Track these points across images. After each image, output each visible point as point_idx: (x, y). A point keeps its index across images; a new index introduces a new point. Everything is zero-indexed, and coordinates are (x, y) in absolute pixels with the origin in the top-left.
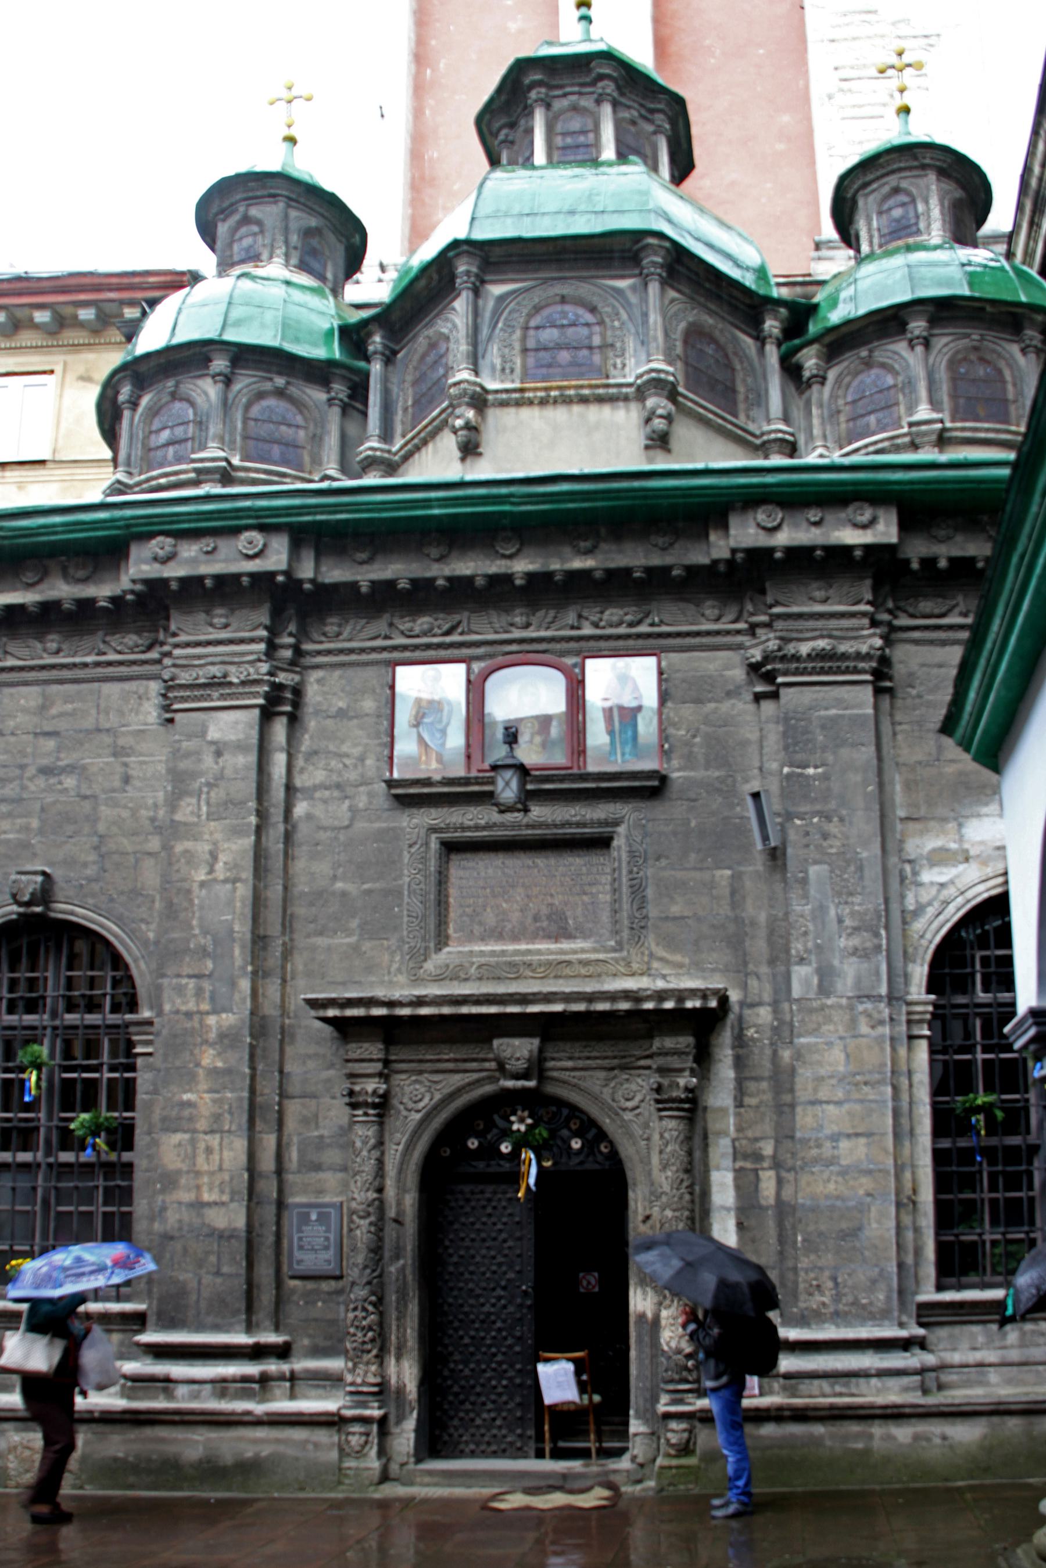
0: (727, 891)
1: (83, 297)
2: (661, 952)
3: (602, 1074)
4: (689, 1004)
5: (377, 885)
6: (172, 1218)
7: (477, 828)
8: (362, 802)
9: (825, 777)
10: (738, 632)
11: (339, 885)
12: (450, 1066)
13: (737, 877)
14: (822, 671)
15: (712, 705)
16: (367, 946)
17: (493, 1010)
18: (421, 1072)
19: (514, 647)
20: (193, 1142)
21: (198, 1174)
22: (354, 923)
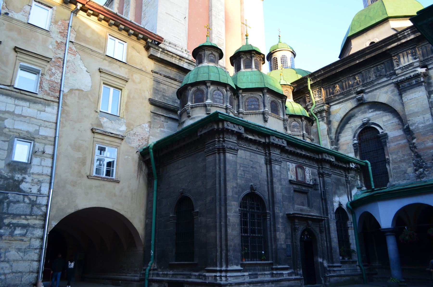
0: (318, 203)
1: (142, 33)
2: (314, 210)
3: (315, 227)
4: (325, 219)
5: (289, 195)
6: (279, 246)
7: (297, 189)
8: (286, 182)
9: (328, 189)
10: (317, 167)
11: (285, 194)
12: (302, 224)
13: (319, 201)
14: (328, 176)
15: (315, 177)
16: (289, 204)
17: (310, 217)
18: (300, 225)
19: (298, 163)
20: (280, 233)
21: (281, 239)
22: (287, 200)
